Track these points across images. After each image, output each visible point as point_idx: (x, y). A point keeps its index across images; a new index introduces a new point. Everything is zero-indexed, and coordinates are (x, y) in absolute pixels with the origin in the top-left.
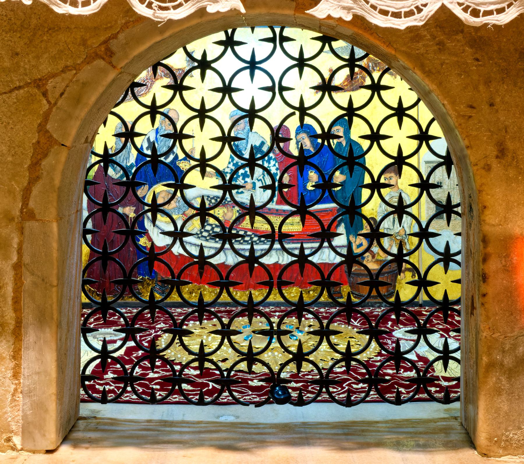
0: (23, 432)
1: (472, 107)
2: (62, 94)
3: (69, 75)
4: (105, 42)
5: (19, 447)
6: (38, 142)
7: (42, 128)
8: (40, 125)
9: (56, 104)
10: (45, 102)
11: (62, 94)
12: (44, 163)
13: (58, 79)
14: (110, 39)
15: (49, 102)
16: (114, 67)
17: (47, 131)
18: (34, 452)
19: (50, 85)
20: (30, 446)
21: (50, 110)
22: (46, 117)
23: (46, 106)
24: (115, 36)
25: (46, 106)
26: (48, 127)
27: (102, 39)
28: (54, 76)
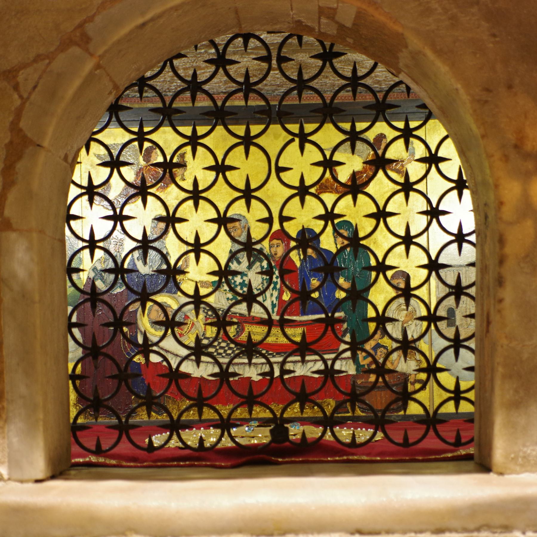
0: (9, 462)
1: (488, 90)
2: (35, 87)
3: (41, 65)
4: (81, 26)
5: (6, 476)
6: (11, 143)
7: (15, 128)
8: (12, 123)
9: (28, 98)
10: (16, 96)
11: (35, 87)
12: (20, 166)
13: (30, 70)
14: (85, 22)
15: (21, 97)
16: (91, 55)
17: (21, 130)
18: (22, 482)
19: (21, 78)
20: (18, 475)
21: (23, 105)
22: (19, 113)
23: (18, 102)
24: (91, 19)
25: (18, 102)
26: (22, 124)
27: (77, 22)
28: (24, 66)
